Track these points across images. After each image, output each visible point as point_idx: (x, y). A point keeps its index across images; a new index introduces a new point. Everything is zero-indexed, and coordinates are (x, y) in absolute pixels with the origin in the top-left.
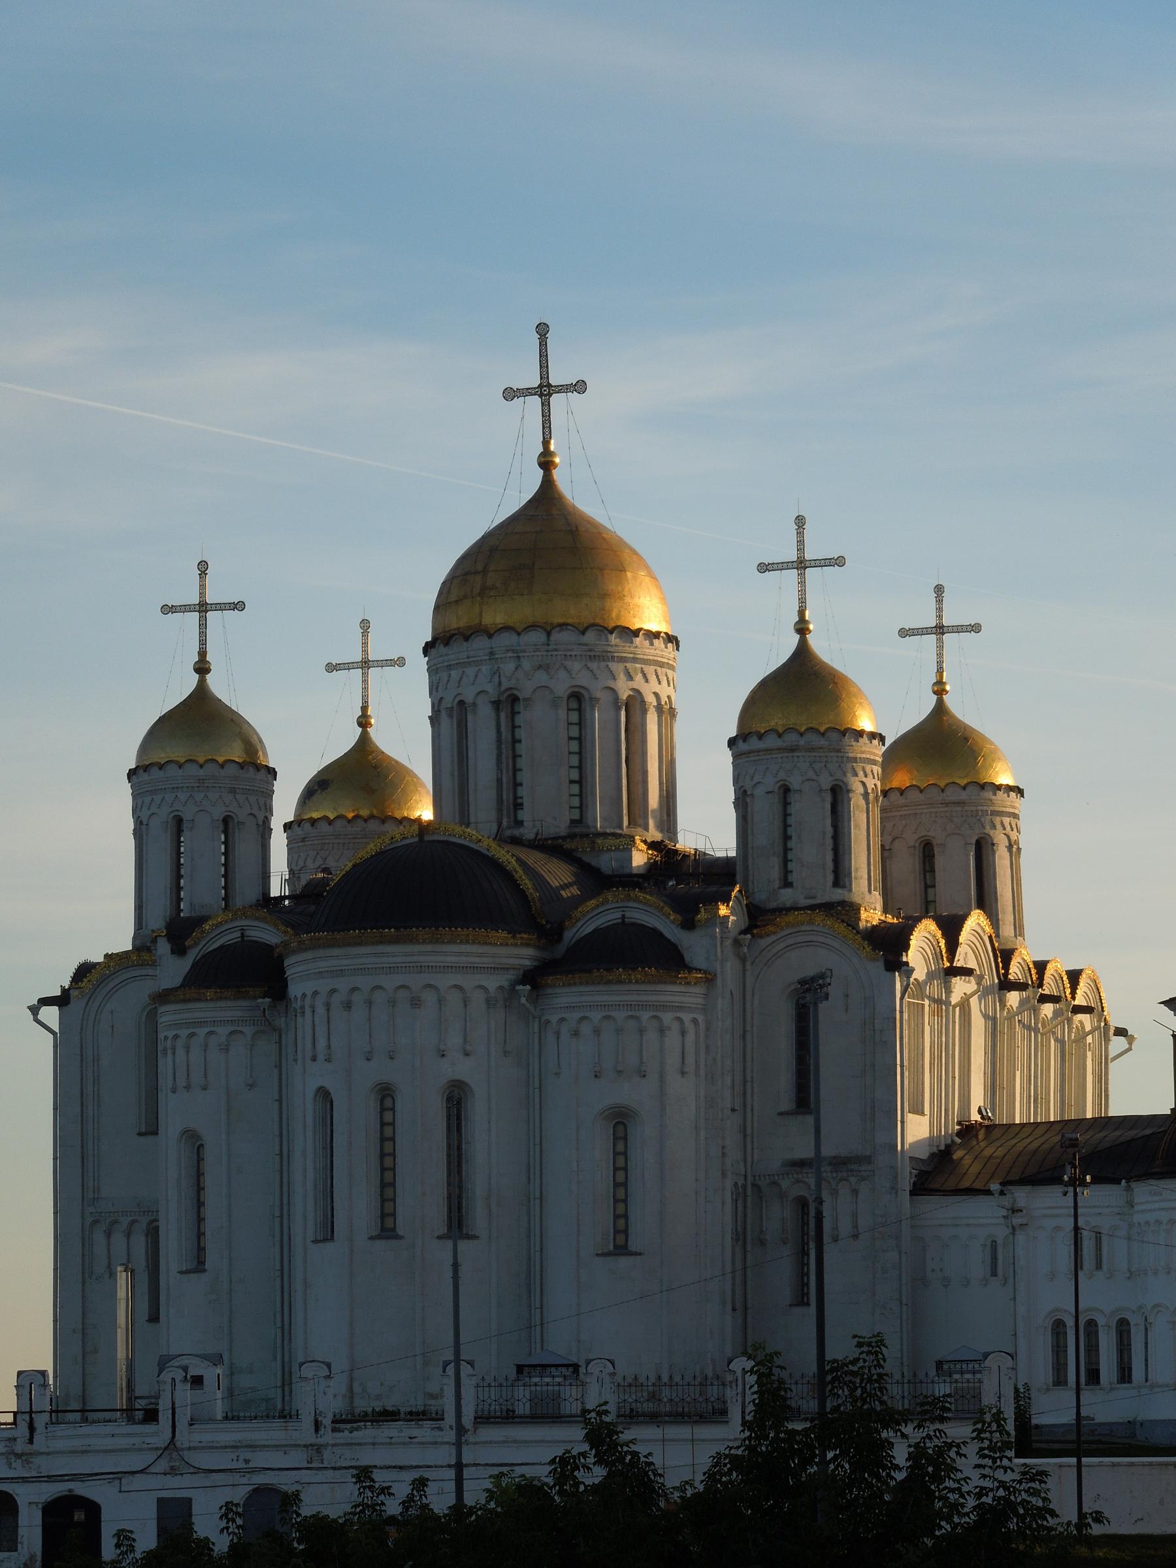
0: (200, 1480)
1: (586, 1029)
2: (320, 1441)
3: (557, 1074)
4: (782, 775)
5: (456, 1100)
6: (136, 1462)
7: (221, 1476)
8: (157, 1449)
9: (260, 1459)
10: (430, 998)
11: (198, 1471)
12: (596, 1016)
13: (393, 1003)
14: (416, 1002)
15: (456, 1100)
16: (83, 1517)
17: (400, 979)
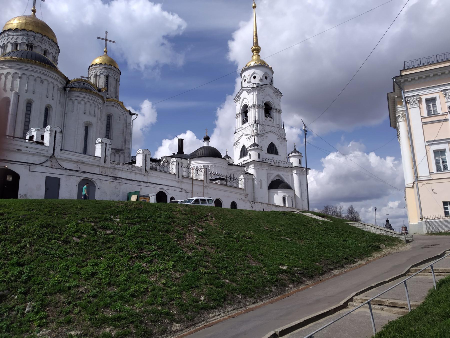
0: (63, 172)
1: (83, 103)
2: (106, 166)
3: (73, 111)
4: (108, 73)
5: (47, 110)
6: (37, 160)
7: (72, 172)
8: (47, 156)
9: (84, 168)
10: (46, 82)
11: (62, 168)
12: (86, 100)
13: (35, 80)
14: (42, 82)
15: (47, 110)
16: (11, 179)
17: (38, 75)
